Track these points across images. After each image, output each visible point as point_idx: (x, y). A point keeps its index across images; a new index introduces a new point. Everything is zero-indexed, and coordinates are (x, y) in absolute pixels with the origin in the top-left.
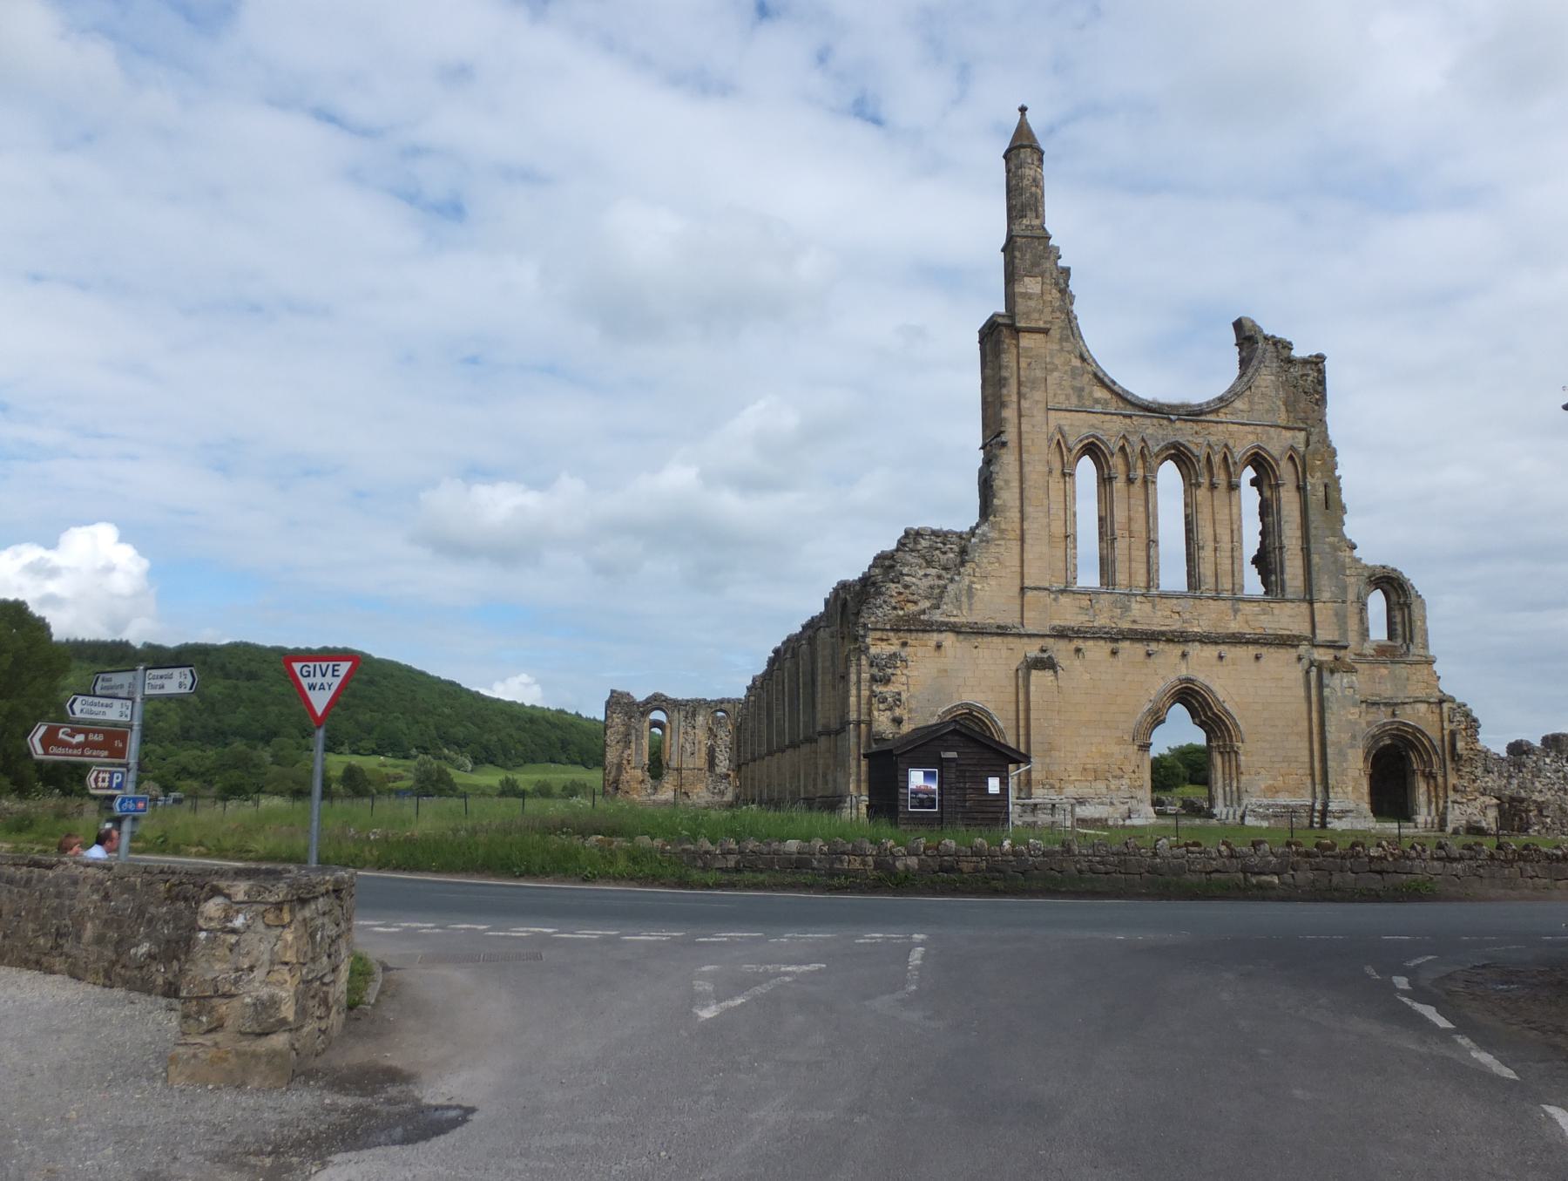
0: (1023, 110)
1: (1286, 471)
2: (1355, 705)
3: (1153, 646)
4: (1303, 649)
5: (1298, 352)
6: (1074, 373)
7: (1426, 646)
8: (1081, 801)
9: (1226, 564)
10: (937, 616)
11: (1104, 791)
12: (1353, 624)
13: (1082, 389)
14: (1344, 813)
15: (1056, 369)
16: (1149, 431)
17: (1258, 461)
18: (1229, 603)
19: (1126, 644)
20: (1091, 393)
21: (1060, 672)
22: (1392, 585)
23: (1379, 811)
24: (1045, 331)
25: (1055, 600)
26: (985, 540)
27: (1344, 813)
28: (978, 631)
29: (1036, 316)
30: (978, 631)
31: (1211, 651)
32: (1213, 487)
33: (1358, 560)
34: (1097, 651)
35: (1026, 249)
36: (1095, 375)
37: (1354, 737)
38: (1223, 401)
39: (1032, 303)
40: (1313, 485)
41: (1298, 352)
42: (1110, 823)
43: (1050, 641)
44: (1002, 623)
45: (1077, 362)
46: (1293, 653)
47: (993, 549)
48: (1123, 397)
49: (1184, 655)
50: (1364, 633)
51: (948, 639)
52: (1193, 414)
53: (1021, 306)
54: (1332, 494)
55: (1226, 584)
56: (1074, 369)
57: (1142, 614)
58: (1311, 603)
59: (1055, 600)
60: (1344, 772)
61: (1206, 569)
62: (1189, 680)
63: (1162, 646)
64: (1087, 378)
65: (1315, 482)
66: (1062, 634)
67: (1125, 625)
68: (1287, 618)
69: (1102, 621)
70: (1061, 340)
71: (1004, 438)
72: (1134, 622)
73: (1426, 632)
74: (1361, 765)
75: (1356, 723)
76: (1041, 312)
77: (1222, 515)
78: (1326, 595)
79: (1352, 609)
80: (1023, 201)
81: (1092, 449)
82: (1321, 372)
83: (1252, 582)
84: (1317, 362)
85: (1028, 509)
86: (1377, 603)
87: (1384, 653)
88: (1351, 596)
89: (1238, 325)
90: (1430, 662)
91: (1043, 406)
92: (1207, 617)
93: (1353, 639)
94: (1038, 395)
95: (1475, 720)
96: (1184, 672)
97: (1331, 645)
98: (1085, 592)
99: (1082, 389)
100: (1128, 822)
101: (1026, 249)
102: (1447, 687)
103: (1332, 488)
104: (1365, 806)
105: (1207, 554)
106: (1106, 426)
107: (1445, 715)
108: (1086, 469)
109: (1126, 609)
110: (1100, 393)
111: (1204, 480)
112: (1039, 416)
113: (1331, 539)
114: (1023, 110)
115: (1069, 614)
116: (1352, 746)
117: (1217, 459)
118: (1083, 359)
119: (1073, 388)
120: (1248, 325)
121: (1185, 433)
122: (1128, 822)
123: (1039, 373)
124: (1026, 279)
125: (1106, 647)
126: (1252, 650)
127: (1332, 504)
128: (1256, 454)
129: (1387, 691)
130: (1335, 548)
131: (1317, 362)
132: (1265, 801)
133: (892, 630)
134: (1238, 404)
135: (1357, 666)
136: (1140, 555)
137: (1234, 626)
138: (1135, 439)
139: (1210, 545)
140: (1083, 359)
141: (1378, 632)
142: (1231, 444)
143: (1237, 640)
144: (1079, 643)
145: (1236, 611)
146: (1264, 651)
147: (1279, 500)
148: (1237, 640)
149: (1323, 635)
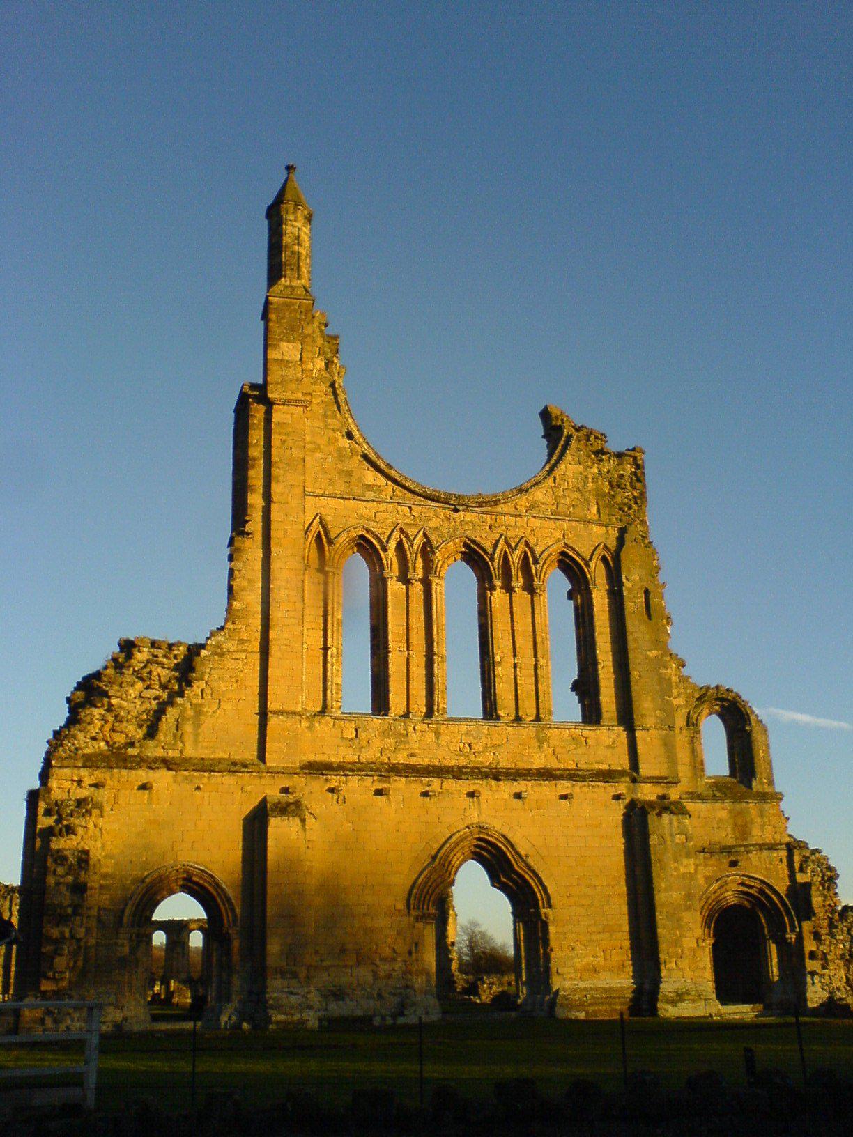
0: (289, 168)
1: (597, 573)
2: (688, 856)
3: (435, 784)
4: (622, 788)
6: (341, 455)
7: (771, 782)
9: (526, 685)
10: (154, 750)
11: (370, 978)
12: (683, 755)
13: (350, 473)
14: (680, 997)
15: (318, 448)
16: (433, 524)
17: (569, 565)
19: (399, 784)
20: (360, 479)
21: (310, 821)
23: (726, 993)
24: (303, 404)
25: (310, 728)
26: (220, 653)
27: (680, 997)
28: (205, 766)
29: (294, 386)
30: (205, 766)
31: (507, 788)
33: (684, 679)
37: (689, 896)
39: (290, 373)
40: (630, 590)
42: (377, 1021)
43: (299, 782)
44: (237, 757)
45: (346, 443)
46: (612, 789)
47: (230, 664)
50: (698, 766)
51: (161, 779)
52: (485, 503)
53: (275, 374)
54: (654, 600)
55: (528, 709)
56: (340, 450)
57: (423, 745)
59: (310, 728)
60: (677, 942)
61: (503, 689)
63: (450, 784)
64: (357, 459)
66: (317, 769)
67: (401, 758)
68: (606, 746)
69: (368, 755)
70: (325, 415)
71: (248, 528)
72: (412, 755)
73: (770, 763)
74: (699, 932)
75: (692, 877)
76: (300, 381)
77: (523, 625)
78: (650, 722)
79: (681, 738)
81: (366, 547)
83: (567, 707)
85: (275, 614)
86: (714, 732)
87: (719, 790)
88: (680, 721)
89: (545, 415)
90: (777, 797)
91: (298, 491)
92: (505, 744)
93: (684, 772)
94: (293, 478)
95: (830, 868)
97: (657, 780)
98: (348, 717)
99: (350, 473)
100: (401, 1020)
102: (797, 830)
104: (708, 984)
105: (503, 672)
106: (380, 517)
107: (797, 866)
108: (359, 568)
109: (402, 738)
110: (371, 476)
111: (498, 583)
112: (295, 503)
113: (654, 653)
115: (327, 743)
116: (688, 908)
119: (340, 472)
120: (554, 411)
122: (401, 1020)
123: (296, 453)
124: (283, 345)
125: (371, 784)
126: (564, 786)
128: (563, 553)
129: (726, 836)
130: (658, 663)
133: (85, 766)
134: (539, 494)
135: (690, 806)
136: (419, 671)
137: (539, 761)
138: (411, 532)
141: (717, 763)
142: (532, 542)
144: (335, 781)
145: (541, 741)
146: (577, 789)
149: (645, 769)
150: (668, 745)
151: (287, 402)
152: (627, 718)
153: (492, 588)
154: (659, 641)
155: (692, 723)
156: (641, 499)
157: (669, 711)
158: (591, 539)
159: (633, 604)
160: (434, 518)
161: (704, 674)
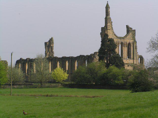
0: (108, 2)
5: (133, 29)
22: (141, 58)
32: (125, 47)
35: (107, 19)
36: (114, 34)
38: (126, 36)
41: (133, 29)
45: (113, 33)
48: (117, 37)
52: (123, 38)
58: (134, 60)
65: (135, 45)
79: (137, 60)
80: (107, 13)
82: (135, 32)
84: (135, 31)
89: (127, 26)
101: (107, 19)
103: (136, 47)
114: (108, 2)
117: (125, 43)
118: (113, 32)
121: (122, 40)
127: (136, 48)
131: (135, 31)
139: (124, 53)
140: (113, 32)
145: (127, 61)
147: (131, 48)
150: (136, 61)
151: (109, 29)
152: (133, 59)
153: (123, 46)
154: (136, 51)
155: (138, 59)
156: (135, 36)
157: (136, 58)
158: (131, 41)
159: (135, 48)
160: (119, 40)
161: (140, 54)
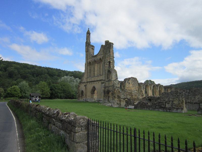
0: (89, 29)
8: (88, 99)
18: (97, 77)
30: (83, 83)
34: (89, 83)
49: (94, 83)
51: (82, 84)
62: (94, 86)
66: (87, 82)
78: (104, 74)
96: (94, 85)
97: (104, 80)
114: (89, 29)
126: (98, 82)
132: (99, 99)
137: (98, 79)
143: (97, 81)
148: (97, 81)
160: (93, 59)
